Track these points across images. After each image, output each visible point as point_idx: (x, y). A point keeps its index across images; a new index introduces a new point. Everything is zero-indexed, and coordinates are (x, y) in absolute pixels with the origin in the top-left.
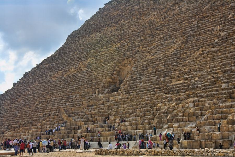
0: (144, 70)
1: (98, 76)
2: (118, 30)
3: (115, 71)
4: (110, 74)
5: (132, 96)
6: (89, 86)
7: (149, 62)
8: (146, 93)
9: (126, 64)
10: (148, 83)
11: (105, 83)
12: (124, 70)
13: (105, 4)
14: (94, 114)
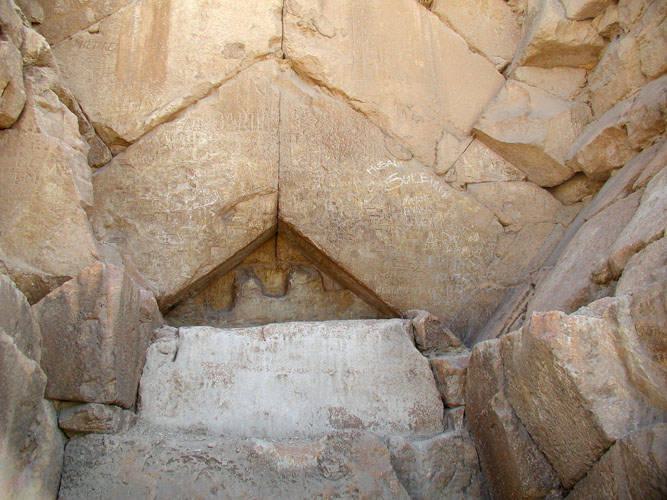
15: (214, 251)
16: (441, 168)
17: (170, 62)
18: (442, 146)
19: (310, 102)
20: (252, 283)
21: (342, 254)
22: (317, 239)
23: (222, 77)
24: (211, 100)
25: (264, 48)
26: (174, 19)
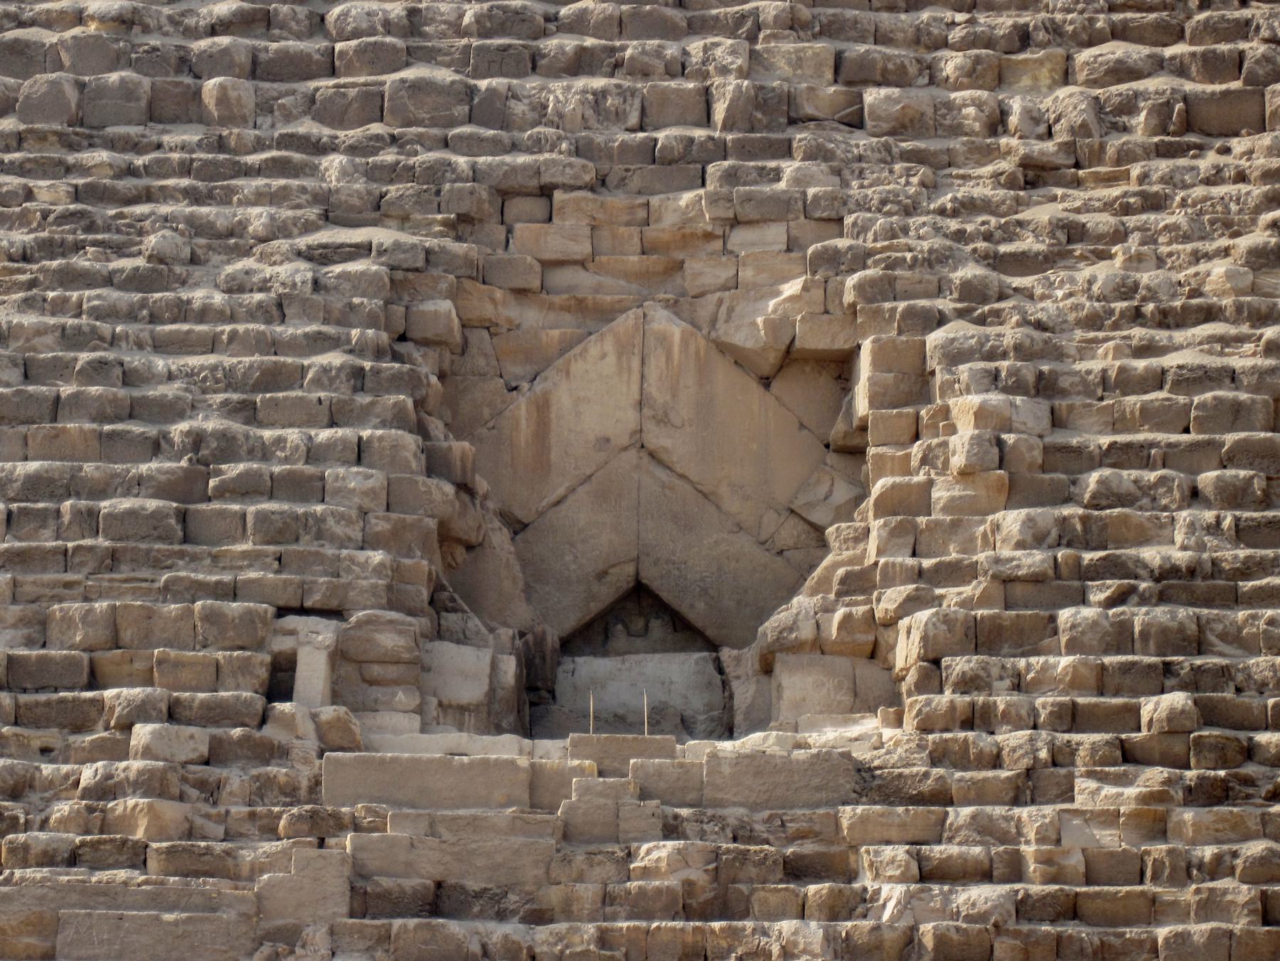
1: (129, 377)
12: (541, 362)
15: (592, 605)
16: (763, 537)
17: (554, 456)
18: (765, 520)
19: (663, 486)
20: (620, 627)
21: (684, 609)
22: (664, 595)
23: (594, 468)
24: (586, 487)
25: (625, 441)
26: (553, 416)
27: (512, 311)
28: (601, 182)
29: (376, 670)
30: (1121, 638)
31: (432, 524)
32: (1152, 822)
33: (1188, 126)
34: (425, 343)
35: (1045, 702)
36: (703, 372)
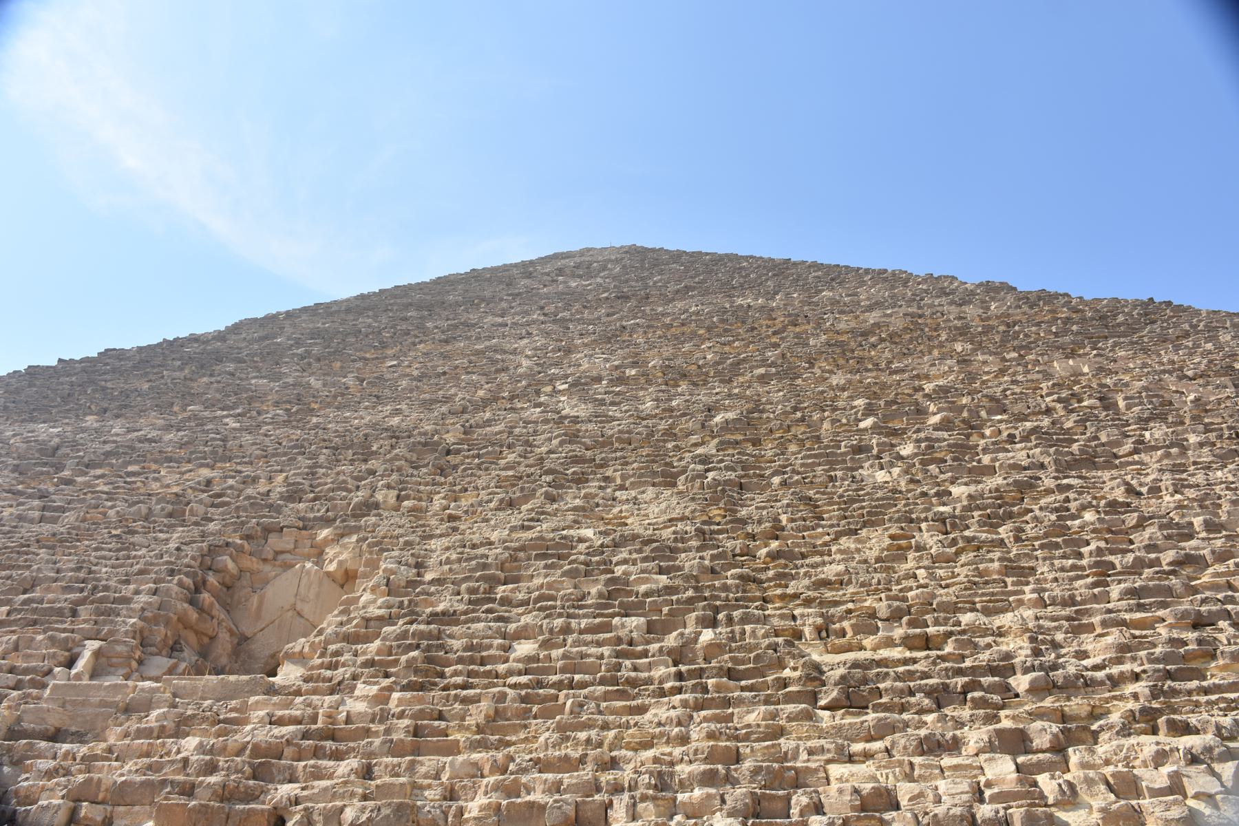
0: (493, 582)
1: (90, 572)
2: (178, 430)
3: (211, 573)
4: (187, 574)
5: (485, 705)
6: (9, 614)
7: (515, 550)
8: (622, 695)
9: (282, 552)
10: (599, 644)
11: (155, 620)
12: (266, 582)
13: (60, 360)
14: (101, 796)
27: (261, 566)
28: (305, 528)
29: (114, 660)
30: (404, 635)
31: (176, 618)
32: (382, 698)
33: (511, 504)
34: (217, 571)
35: (360, 659)
36: (320, 583)
